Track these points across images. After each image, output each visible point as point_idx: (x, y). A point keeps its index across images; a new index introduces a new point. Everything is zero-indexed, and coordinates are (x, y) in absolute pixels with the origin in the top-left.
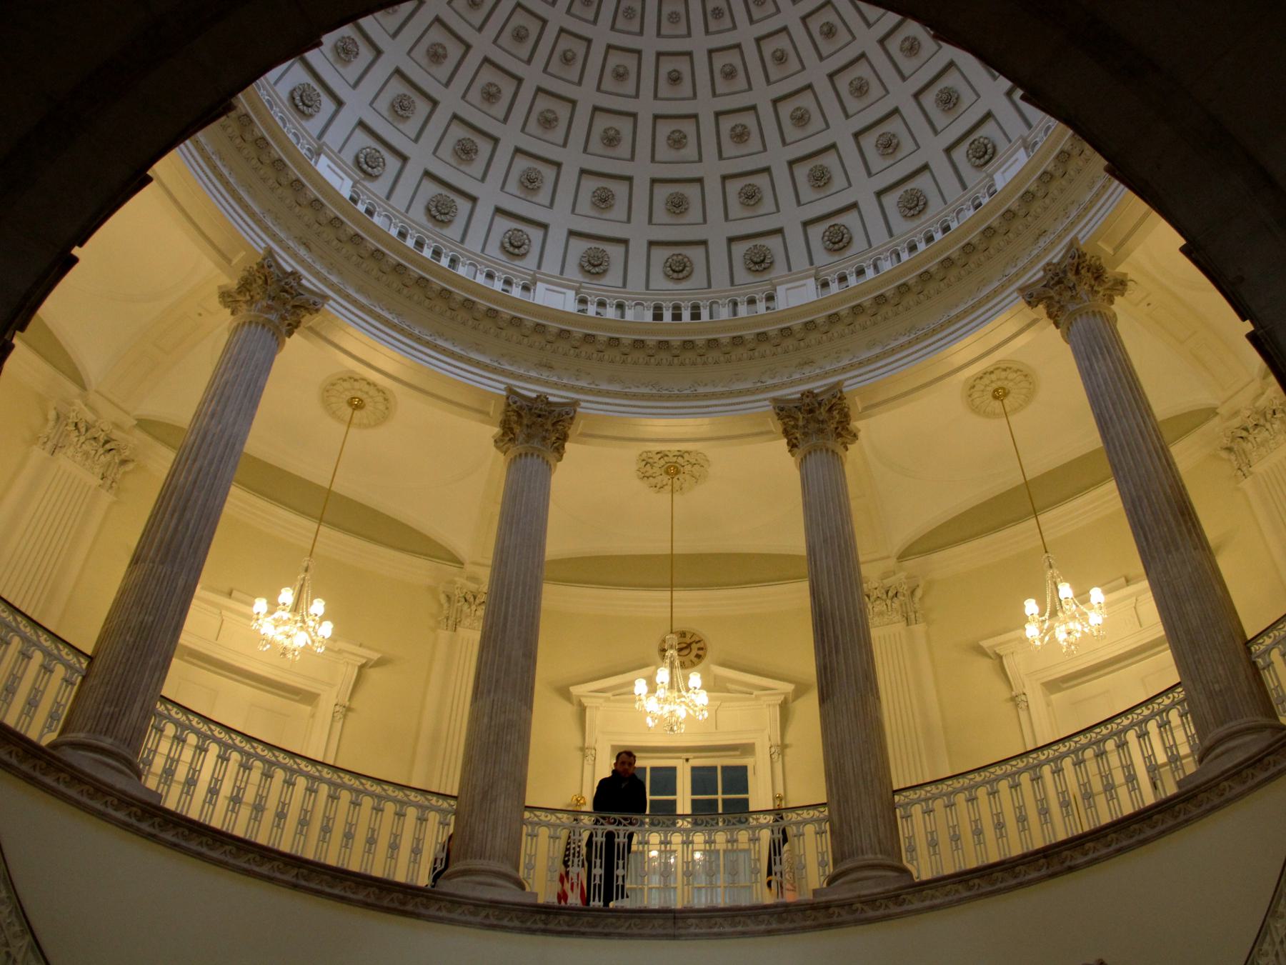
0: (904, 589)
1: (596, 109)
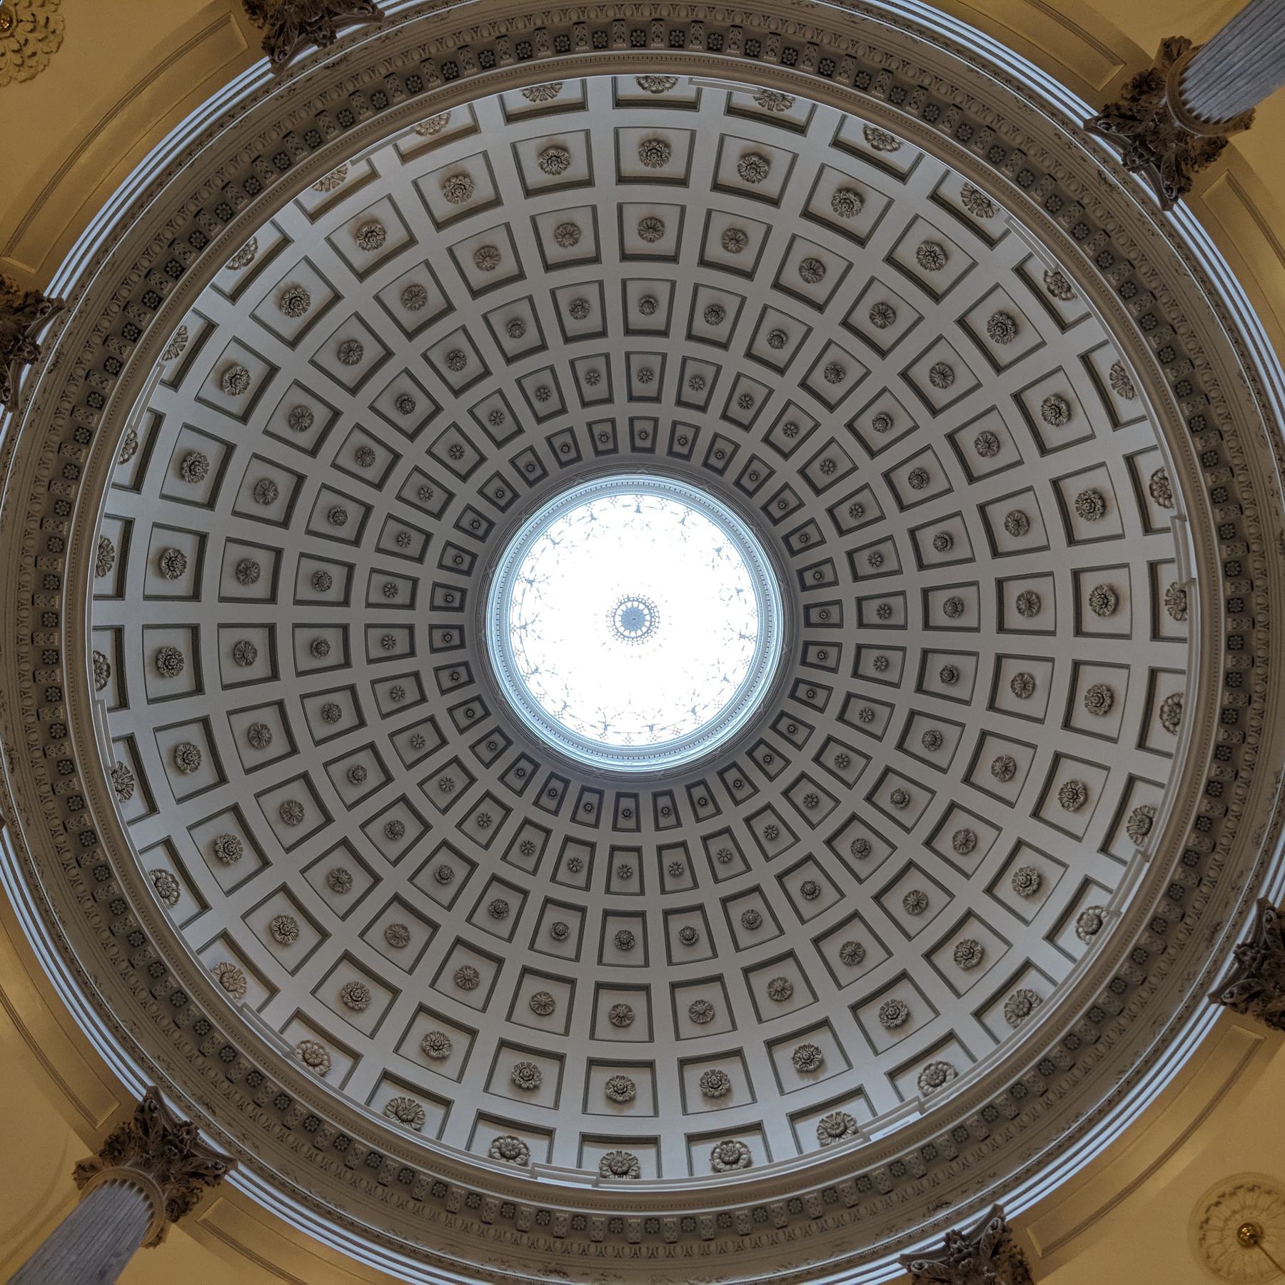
1: (967, 780)
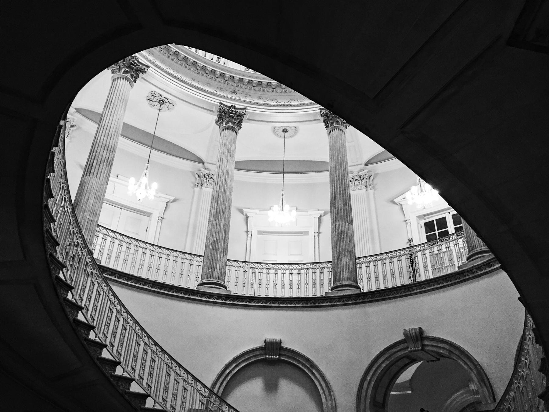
0: (366, 177)
